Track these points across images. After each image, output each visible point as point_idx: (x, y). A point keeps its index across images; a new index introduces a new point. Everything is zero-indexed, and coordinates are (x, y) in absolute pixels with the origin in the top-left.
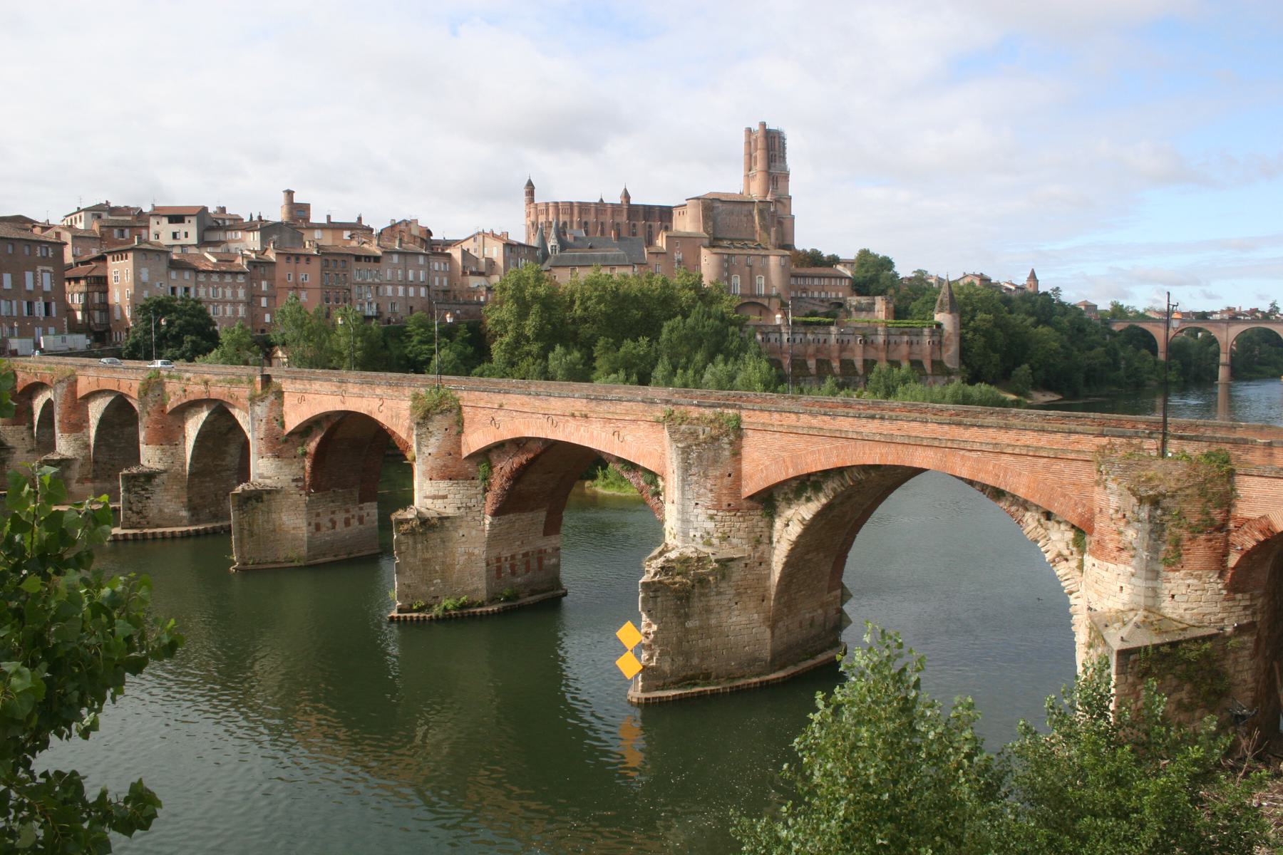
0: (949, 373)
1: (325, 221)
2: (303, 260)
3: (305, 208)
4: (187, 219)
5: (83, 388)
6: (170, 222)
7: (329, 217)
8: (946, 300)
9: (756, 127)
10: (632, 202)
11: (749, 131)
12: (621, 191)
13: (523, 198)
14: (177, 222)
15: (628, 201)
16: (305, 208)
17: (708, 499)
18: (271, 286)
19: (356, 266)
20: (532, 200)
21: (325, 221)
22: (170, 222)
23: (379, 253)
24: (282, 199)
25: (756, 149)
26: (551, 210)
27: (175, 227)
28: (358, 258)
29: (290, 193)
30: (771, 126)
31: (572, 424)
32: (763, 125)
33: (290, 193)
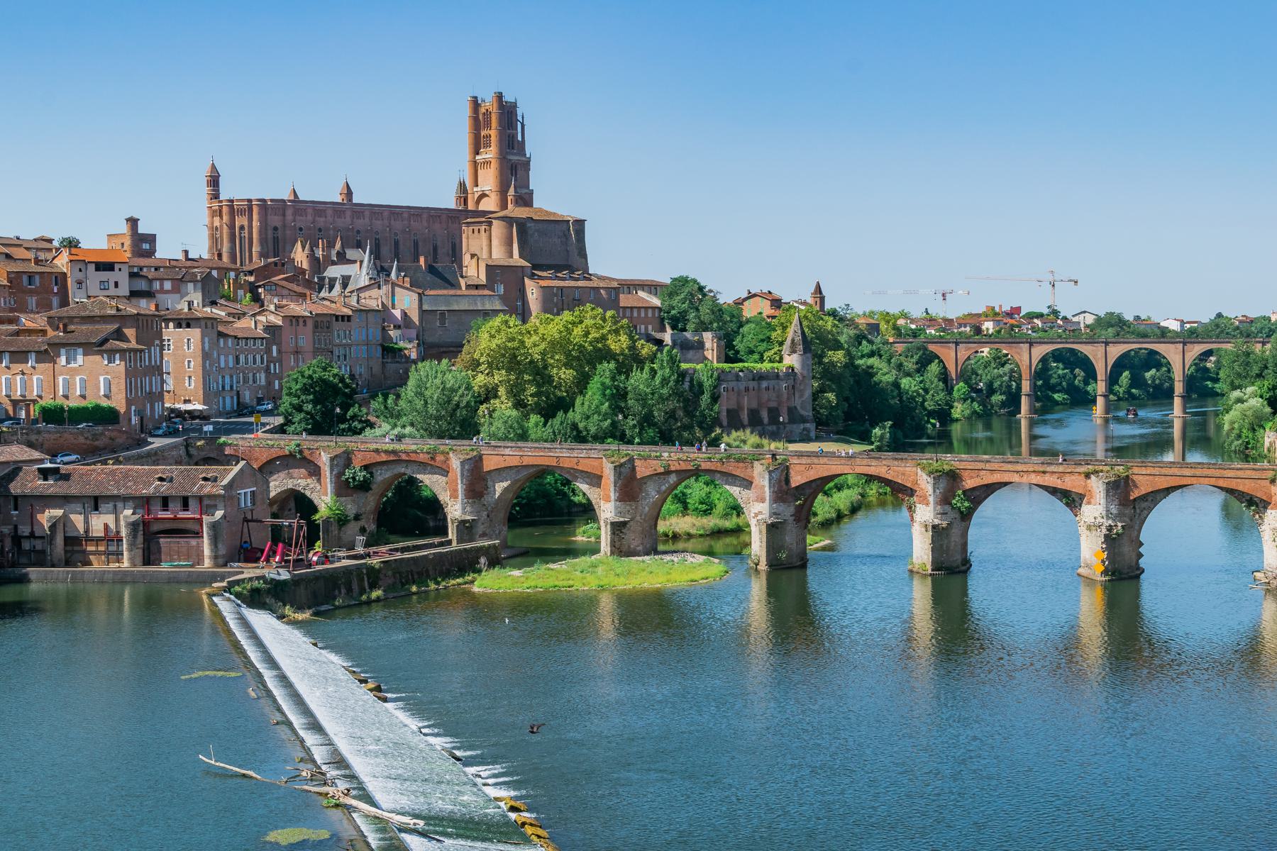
0: (804, 420)
1: (181, 256)
2: (301, 321)
3: (151, 239)
4: (117, 267)
5: (490, 464)
6: (97, 269)
7: (186, 252)
8: (799, 338)
9: (489, 103)
10: (355, 201)
11: (476, 104)
12: (340, 186)
13: (205, 190)
14: (104, 270)
15: (351, 200)
16: (151, 239)
17: (1116, 502)
18: (279, 351)
19: (337, 326)
20: (215, 196)
21: (181, 256)
22: (97, 269)
23: (347, 312)
24: (124, 228)
25: (489, 126)
26: (255, 210)
27: (104, 275)
28: (337, 317)
29: (133, 222)
30: (508, 98)
31: (1033, 476)
32: (500, 96)
33: (133, 222)
